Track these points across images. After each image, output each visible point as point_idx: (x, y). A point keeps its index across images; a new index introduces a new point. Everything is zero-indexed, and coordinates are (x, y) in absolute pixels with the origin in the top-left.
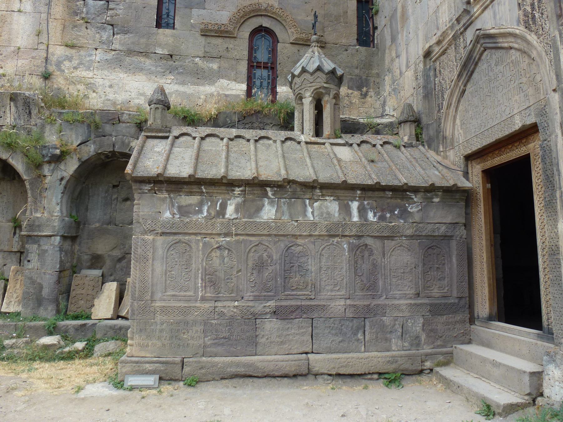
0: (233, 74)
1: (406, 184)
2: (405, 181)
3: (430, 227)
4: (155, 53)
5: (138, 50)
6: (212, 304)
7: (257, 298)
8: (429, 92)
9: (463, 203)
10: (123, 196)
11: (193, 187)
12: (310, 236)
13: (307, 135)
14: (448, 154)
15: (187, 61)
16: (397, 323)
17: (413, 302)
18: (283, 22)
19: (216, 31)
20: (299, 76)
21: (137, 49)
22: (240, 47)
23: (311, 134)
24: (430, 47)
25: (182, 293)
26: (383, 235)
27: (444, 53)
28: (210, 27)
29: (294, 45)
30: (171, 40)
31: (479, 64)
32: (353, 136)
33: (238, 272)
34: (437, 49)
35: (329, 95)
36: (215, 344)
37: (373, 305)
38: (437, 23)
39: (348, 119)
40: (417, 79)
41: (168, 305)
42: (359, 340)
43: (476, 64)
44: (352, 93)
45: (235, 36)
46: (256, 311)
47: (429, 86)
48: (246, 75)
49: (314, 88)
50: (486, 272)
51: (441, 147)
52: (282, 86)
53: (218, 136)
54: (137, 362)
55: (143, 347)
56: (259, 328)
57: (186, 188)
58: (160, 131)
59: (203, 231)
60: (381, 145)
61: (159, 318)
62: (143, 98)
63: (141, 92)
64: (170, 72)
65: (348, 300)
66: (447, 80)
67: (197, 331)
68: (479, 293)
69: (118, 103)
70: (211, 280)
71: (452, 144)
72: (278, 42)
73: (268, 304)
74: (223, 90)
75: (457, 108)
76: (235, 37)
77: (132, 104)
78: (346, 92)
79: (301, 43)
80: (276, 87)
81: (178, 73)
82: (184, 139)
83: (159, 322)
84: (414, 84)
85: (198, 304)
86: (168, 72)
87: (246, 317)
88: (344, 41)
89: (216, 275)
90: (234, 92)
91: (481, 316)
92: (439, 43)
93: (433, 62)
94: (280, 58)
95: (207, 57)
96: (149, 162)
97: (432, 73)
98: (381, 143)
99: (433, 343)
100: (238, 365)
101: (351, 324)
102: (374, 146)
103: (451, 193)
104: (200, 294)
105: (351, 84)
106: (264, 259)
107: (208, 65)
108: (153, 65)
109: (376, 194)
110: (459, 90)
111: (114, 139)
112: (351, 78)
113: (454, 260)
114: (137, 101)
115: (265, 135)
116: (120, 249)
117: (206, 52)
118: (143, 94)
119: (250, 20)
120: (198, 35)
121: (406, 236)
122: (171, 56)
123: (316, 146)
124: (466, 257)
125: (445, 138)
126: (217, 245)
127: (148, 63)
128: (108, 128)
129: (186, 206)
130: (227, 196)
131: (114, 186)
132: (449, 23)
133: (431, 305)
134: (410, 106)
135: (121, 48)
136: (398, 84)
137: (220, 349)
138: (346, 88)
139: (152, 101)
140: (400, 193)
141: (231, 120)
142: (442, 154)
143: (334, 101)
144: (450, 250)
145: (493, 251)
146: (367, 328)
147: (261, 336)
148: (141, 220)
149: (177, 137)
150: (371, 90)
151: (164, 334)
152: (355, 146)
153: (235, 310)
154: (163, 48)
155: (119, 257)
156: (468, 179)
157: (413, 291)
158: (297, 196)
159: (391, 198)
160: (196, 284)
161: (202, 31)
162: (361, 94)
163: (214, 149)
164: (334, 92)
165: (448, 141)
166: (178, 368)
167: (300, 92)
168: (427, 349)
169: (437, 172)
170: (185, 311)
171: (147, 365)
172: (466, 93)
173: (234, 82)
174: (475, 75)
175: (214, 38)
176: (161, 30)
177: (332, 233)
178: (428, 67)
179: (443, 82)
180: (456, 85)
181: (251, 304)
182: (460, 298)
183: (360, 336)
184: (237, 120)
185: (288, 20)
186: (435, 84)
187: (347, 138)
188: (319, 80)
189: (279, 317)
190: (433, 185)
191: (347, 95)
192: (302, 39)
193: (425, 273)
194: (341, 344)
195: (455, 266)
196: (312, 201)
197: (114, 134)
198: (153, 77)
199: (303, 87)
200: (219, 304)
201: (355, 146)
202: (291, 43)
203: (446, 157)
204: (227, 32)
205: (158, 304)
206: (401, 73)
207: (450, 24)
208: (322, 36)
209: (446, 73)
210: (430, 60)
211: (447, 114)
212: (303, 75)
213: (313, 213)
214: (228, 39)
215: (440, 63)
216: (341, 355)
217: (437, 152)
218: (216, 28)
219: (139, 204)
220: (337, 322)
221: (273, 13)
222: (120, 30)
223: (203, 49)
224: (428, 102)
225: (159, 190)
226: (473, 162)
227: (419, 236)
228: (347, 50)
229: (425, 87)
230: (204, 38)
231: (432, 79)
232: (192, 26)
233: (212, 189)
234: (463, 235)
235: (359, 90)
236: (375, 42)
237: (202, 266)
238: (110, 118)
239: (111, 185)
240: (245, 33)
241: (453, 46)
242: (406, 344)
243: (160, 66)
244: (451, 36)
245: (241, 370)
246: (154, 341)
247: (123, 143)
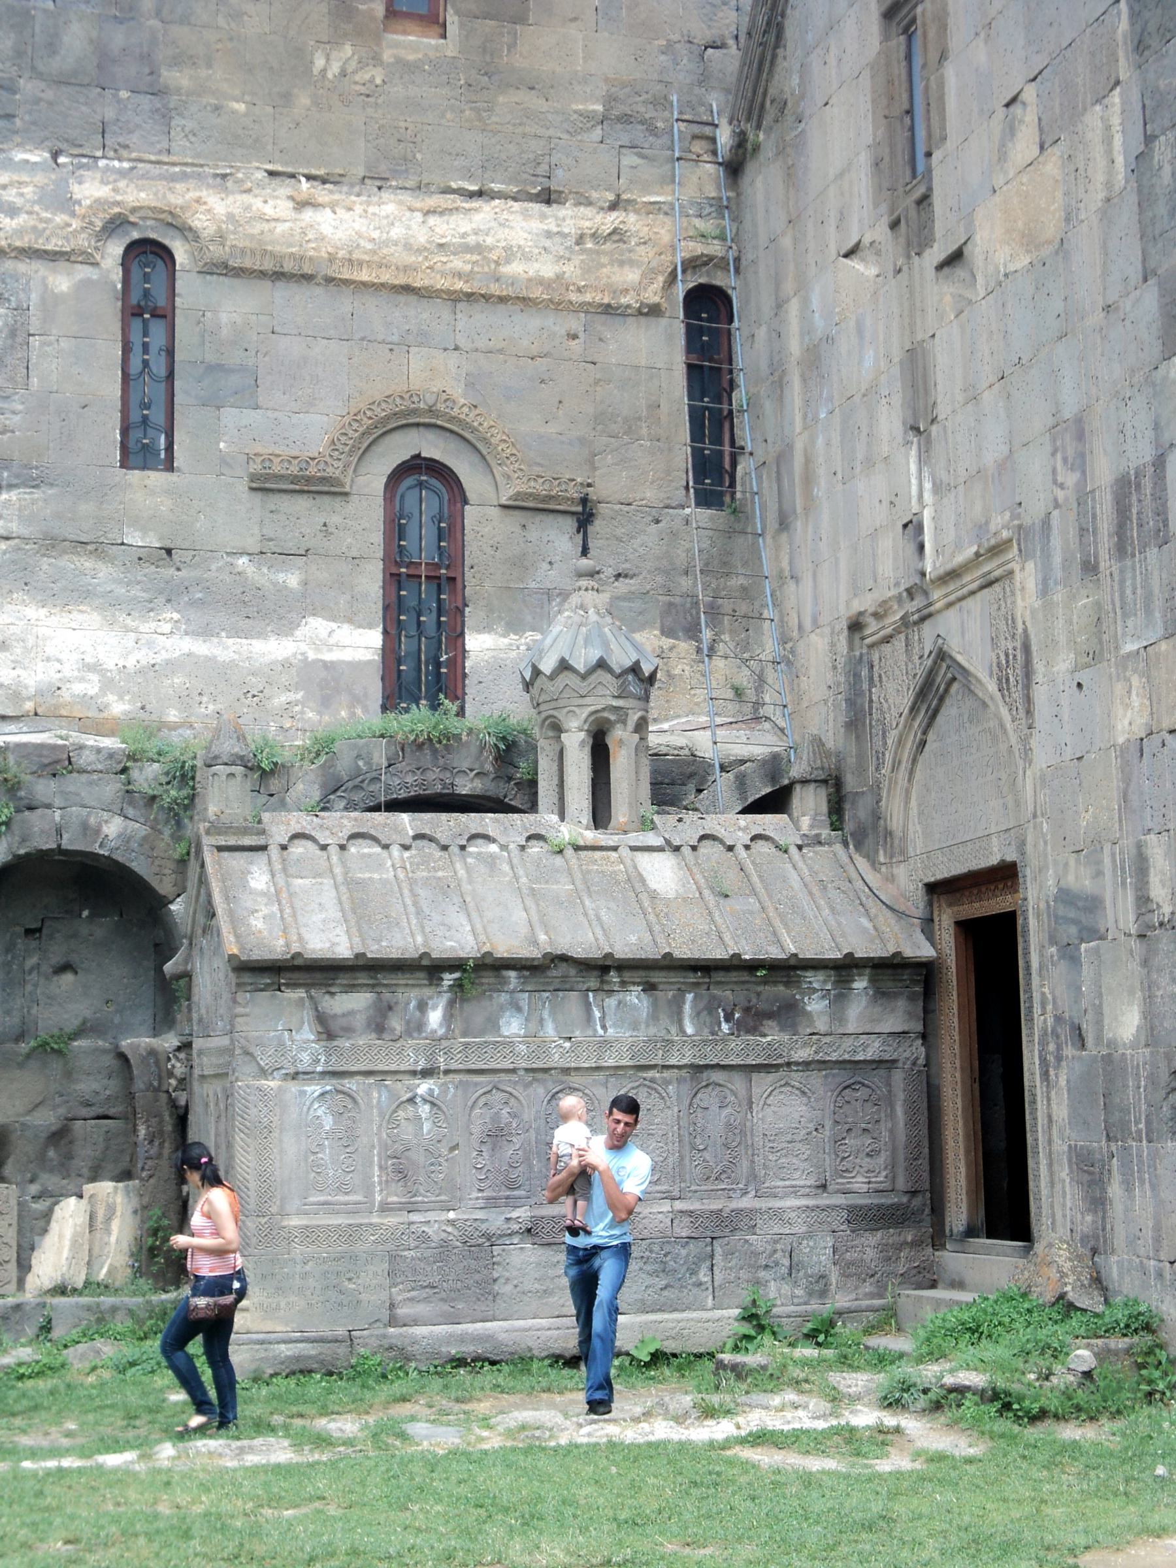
0: (343, 600)
1: (796, 955)
2: (794, 951)
3: (848, 1043)
5: (73, 537)
6: (404, 1217)
7: (492, 1203)
8: (858, 719)
9: (918, 989)
10: (56, 959)
11: (358, 975)
12: (598, 1068)
13: (575, 827)
14: (895, 871)
15: (213, 567)
16: (779, 1246)
17: (811, 1202)
18: (480, 446)
19: (295, 479)
20: (551, 678)
21: (70, 532)
22: (362, 521)
23: (585, 822)
24: (861, 614)
25: (342, 1198)
26: (750, 1061)
27: (887, 640)
28: (277, 469)
29: (512, 512)
30: (164, 505)
31: (948, 701)
32: (680, 820)
33: (452, 1149)
34: (872, 626)
35: (624, 722)
36: (411, 1299)
37: (727, 1210)
39: (664, 750)
40: (835, 668)
41: (314, 1222)
42: (701, 1284)
43: (942, 699)
44: (671, 649)
45: (347, 489)
46: (492, 1230)
47: (859, 701)
48: (380, 605)
49: (592, 708)
50: (961, 1139)
51: (881, 852)
52: (479, 632)
53: (375, 839)
54: (262, 1342)
55: (269, 1312)
56: (498, 1264)
57: (343, 980)
58: (245, 831)
59: (381, 1067)
60: (747, 847)
61: (298, 1250)
62: (94, 677)
63: (88, 660)
64: (169, 601)
65: (677, 1202)
67: (376, 1274)
68: (952, 1182)
69: (24, 693)
70: (400, 1171)
71: (903, 852)
72: (465, 502)
73: (514, 1215)
74: (318, 650)
75: (911, 773)
76: (346, 494)
77: (65, 695)
78: (656, 643)
79: (531, 505)
80: (462, 634)
81: (192, 603)
82: (300, 850)
83: (299, 1258)
84: (829, 677)
85: (375, 1220)
86: (161, 600)
87: (473, 1242)
88: (651, 494)
89: (407, 1158)
90: (346, 655)
91: (955, 1230)
94: (475, 550)
95: (272, 553)
96: (256, 919)
97: (864, 673)
98: (746, 840)
99: (856, 1288)
100: (462, 1339)
101: (684, 1252)
102: (730, 848)
103: (889, 971)
104: (378, 1198)
105: (669, 621)
106: (504, 1121)
107: (272, 577)
108: (119, 582)
109: (734, 976)
111: (57, 818)
112: (671, 604)
113: (899, 1110)
114: (78, 688)
115: (480, 831)
116: (55, 1107)
117: (265, 539)
118: (94, 668)
119: (388, 439)
120: (242, 486)
121: (797, 1064)
122: (169, 552)
123: (598, 855)
124: (925, 1104)
125: (889, 834)
126: (408, 1095)
127: (102, 573)
128: (44, 789)
129: (344, 1015)
130: (427, 992)
131: (29, 932)
133: (851, 1209)
134: (818, 742)
135: (25, 532)
136: (792, 651)
137: (421, 1309)
138: (657, 632)
139: (216, 757)
140: (784, 973)
141: (368, 763)
142: (883, 869)
143: (637, 736)
144: (890, 1091)
145: (977, 1094)
146: (718, 1258)
147: (502, 1280)
148: (252, 1049)
149: (284, 848)
150: (726, 637)
151: (311, 1282)
152: (686, 850)
153: (450, 1229)
154: (144, 530)
155: (53, 1128)
156: (930, 938)
157: (811, 1182)
158: (568, 986)
159: (765, 983)
160: (368, 1177)
161: (253, 478)
162: (699, 650)
163: (376, 876)
164: (636, 717)
165: (897, 842)
166: (342, 1350)
167: (555, 713)
168: (842, 1301)
169: (865, 922)
170: (352, 1233)
171: (283, 1347)
173: (346, 626)
174: (940, 719)
175: (285, 497)
176: (135, 476)
177: (643, 1062)
178: (857, 653)
179: (885, 705)
180: (908, 725)
181: (480, 1215)
182: (913, 1193)
183: (703, 1276)
184: (385, 763)
185: (493, 440)
186: (871, 701)
187: (666, 822)
188: (600, 691)
189: (536, 1240)
190: (850, 955)
191: (658, 652)
192: (535, 497)
193: (837, 1141)
194: (665, 1293)
195: (901, 1124)
196: (601, 995)
197: (58, 802)
198: (122, 617)
199: (561, 703)
200: (414, 1217)
201: (686, 850)
203: (891, 878)
204: (323, 480)
205: (295, 1221)
206: (800, 627)
208: (589, 485)
209: (890, 686)
210: (863, 639)
211: (893, 782)
212: (561, 676)
213: (603, 1019)
214: (326, 499)
216: (666, 1316)
217: (874, 864)
218: (294, 469)
219: (246, 1015)
220: (656, 1248)
221: (452, 419)
222: (17, 476)
223: (256, 531)
224: (857, 737)
225: (287, 985)
227: (824, 1062)
228: (657, 522)
229: (851, 703)
230: (259, 495)
231: (865, 686)
232: (224, 461)
233: (400, 979)
234: (917, 1058)
235: (691, 638)
236: (738, 495)
237: (380, 1139)
238: (46, 761)
239: (20, 930)
240: (372, 480)
241: (902, 636)
242: (799, 1292)
243: (139, 583)
245: (469, 1349)
246: (292, 1298)
247: (85, 826)
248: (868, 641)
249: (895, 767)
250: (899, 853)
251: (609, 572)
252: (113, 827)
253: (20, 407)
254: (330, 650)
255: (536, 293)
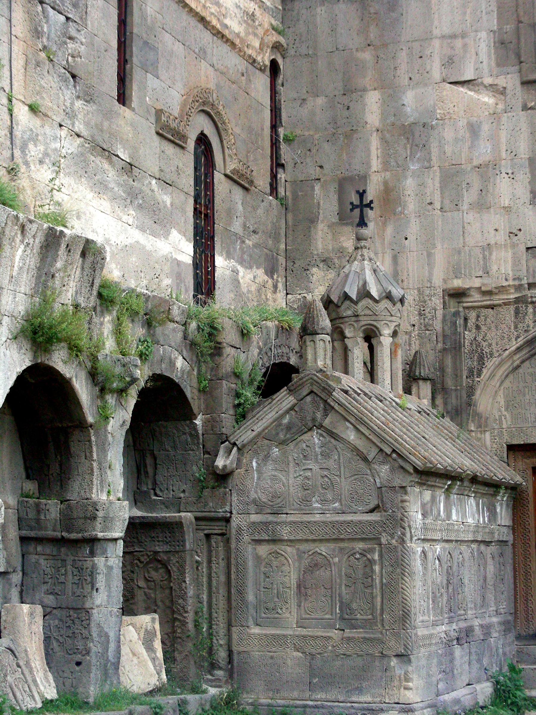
0: (183, 220)
4: (117, 156)
18: (223, 133)
27: (492, 307)
38: (485, 264)
44: (267, 282)
49: (395, 324)
66: (494, 344)
71: (486, 426)
81: (140, 207)
92: (489, 293)
93: (464, 308)
97: (460, 322)
110: (512, 364)
127: (111, 175)
132: (514, 279)
139: (323, 329)
167: (375, 323)
172: (521, 370)
179: (485, 344)
186: (464, 338)
202: (226, 176)
207: (517, 283)
210: (459, 303)
215: (478, 316)
221: (218, 113)
226: (517, 453)
241: (512, 308)
244: (512, 296)
248: (465, 305)
249: (492, 376)
250: (483, 424)
251: (252, 229)
252: (180, 363)
253: (84, 40)
254: (179, 254)
255: (237, 42)
